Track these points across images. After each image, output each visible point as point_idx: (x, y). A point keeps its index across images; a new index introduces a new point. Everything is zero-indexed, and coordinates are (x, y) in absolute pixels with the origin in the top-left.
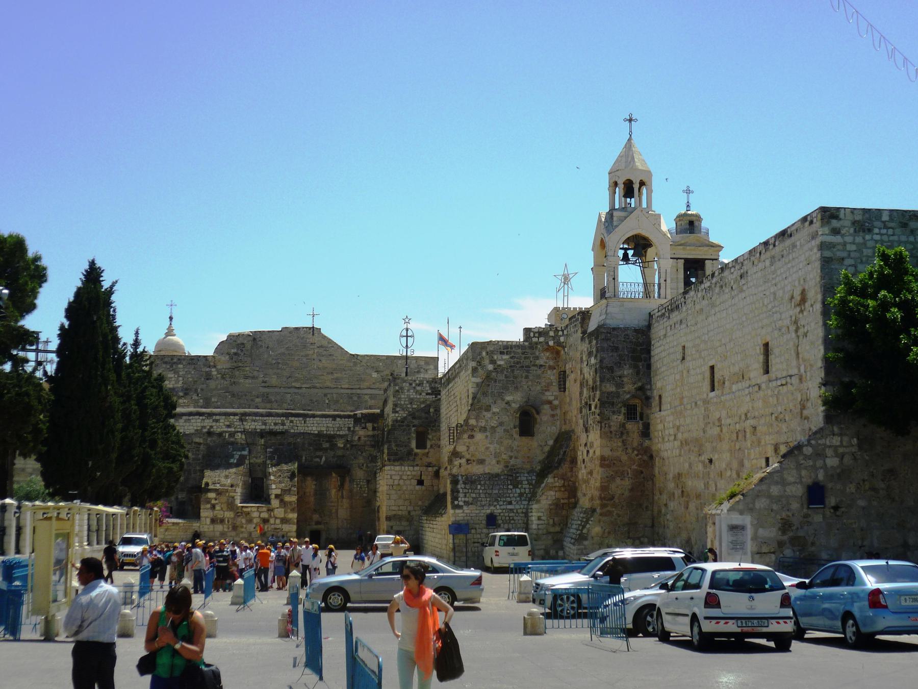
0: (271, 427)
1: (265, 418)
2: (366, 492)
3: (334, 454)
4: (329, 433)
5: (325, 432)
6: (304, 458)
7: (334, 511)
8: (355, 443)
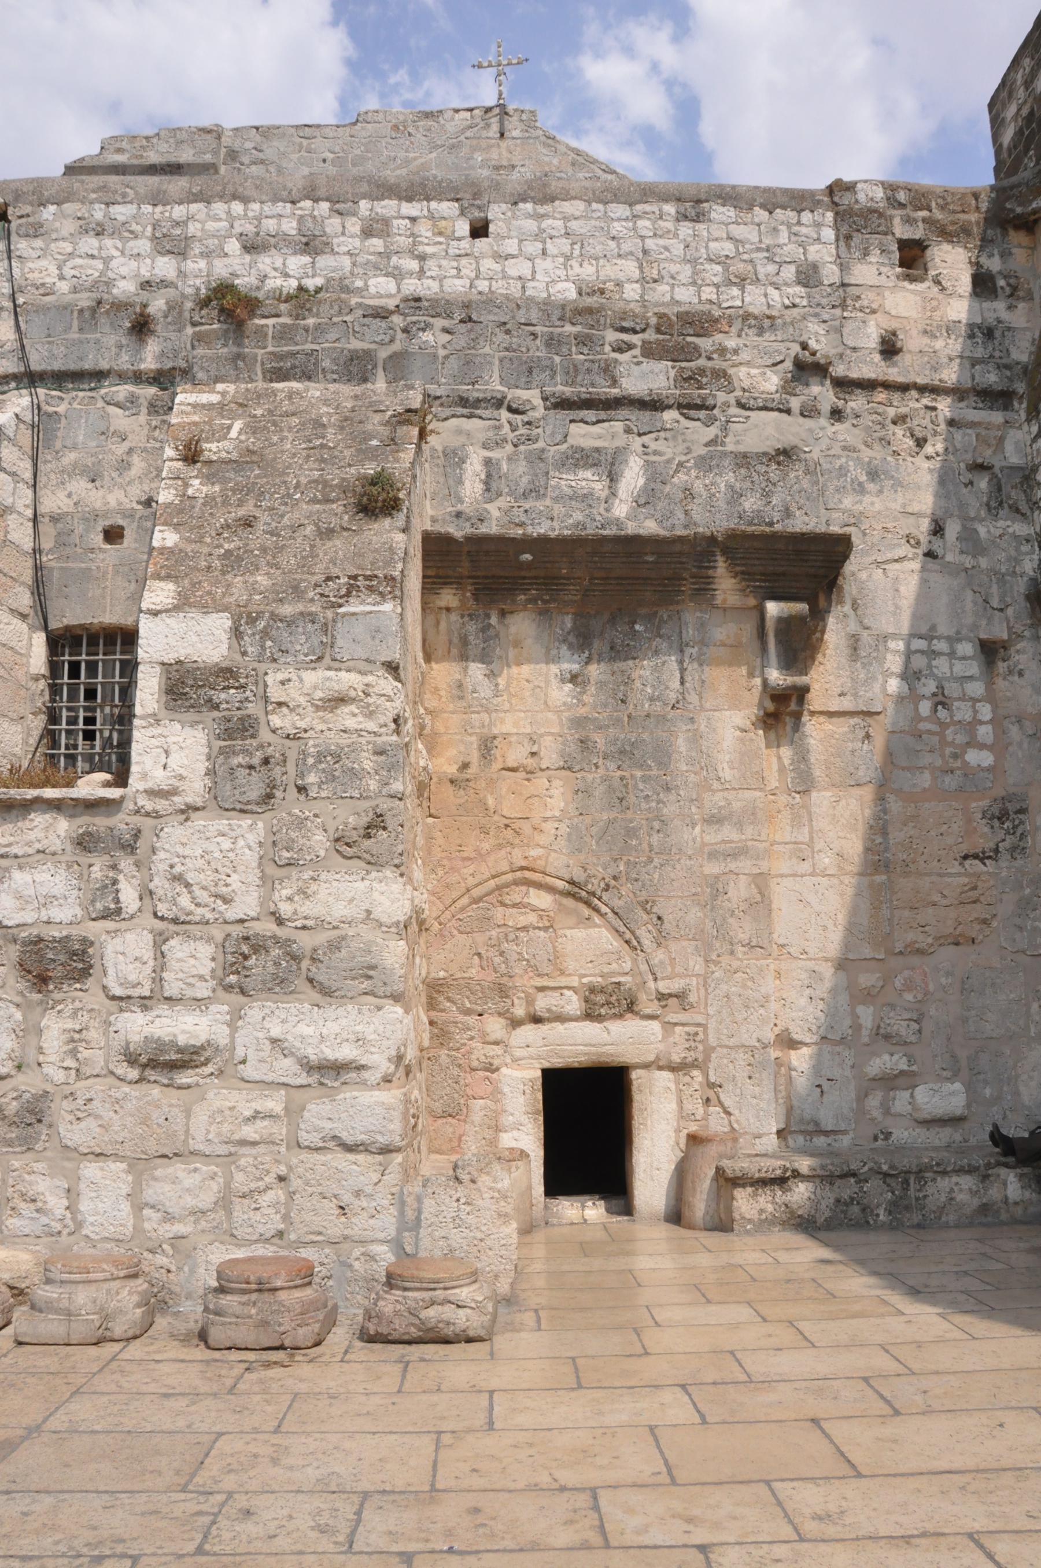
0: (221, 269)
1: (179, 212)
2: (985, 732)
3: (713, 442)
4: (662, 293)
5: (632, 292)
6: (474, 466)
7: (739, 890)
8: (867, 372)
